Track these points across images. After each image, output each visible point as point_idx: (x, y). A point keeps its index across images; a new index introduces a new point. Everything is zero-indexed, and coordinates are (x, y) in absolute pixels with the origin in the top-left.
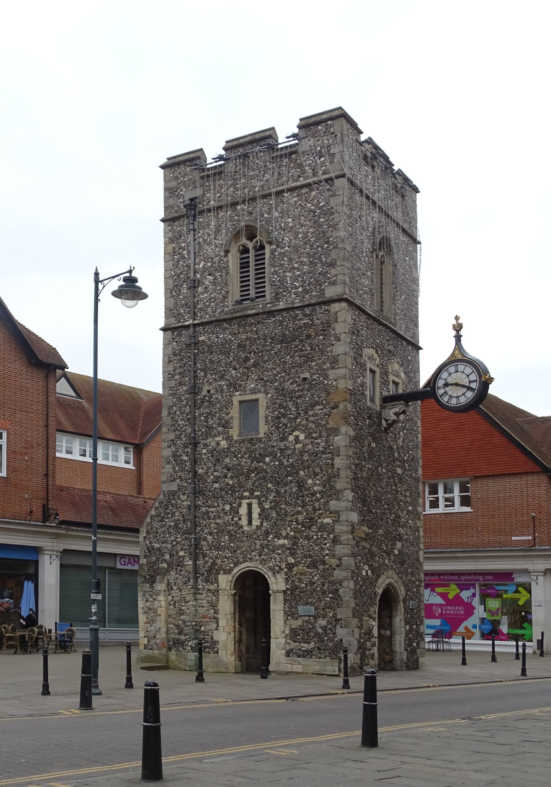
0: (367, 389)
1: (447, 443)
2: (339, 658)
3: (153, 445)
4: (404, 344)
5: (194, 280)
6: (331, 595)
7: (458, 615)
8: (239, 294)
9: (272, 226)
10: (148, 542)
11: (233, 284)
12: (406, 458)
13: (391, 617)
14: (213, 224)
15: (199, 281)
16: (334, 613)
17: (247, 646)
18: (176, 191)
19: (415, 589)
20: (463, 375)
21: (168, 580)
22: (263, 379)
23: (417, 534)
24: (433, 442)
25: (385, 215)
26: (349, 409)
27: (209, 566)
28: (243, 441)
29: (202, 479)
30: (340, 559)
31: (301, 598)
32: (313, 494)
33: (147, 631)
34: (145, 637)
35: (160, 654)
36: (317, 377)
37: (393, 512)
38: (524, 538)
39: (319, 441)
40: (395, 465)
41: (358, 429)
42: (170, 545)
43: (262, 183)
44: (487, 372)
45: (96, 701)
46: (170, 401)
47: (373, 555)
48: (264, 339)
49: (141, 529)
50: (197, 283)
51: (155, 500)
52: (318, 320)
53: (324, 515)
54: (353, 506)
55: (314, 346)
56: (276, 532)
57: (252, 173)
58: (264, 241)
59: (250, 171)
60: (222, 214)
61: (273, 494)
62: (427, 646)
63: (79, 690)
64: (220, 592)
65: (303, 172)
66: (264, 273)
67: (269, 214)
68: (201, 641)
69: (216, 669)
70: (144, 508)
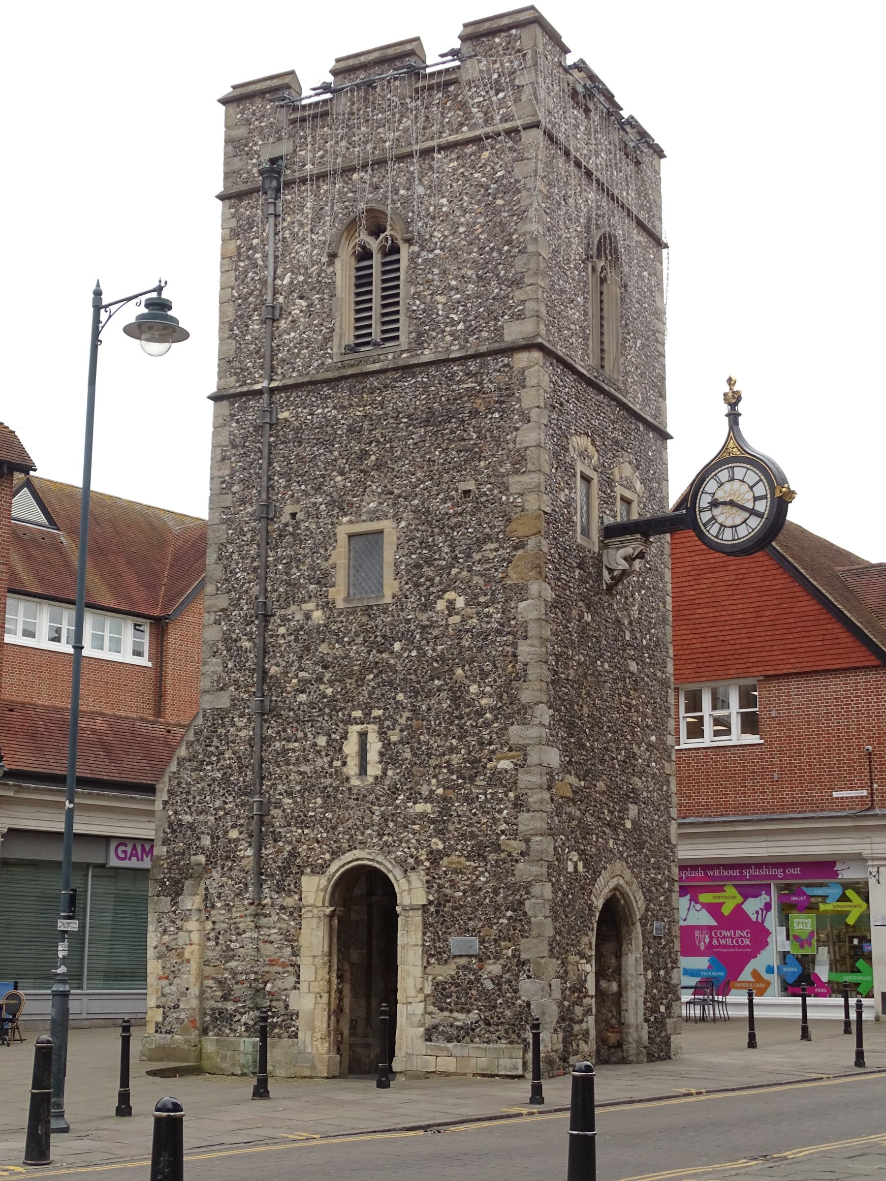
0: (576, 513)
1: (716, 614)
2: (525, 1040)
3: (188, 618)
4: (642, 428)
5: (273, 307)
6: (509, 913)
7: (739, 947)
8: (353, 333)
9: (413, 212)
10: (170, 813)
11: (341, 314)
12: (644, 643)
13: (619, 956)
14: (309, 205)
15: (281, 309)
16: (515, 950)
17: (351, 1021)
18: (246, 145)
19: (662, 898)
20: (743, 487)
21: (206, 889)
22: (392, 493)
23: (665, 788)
24: (692, 612)
25: (608, 194)
26: (545, 550)
27: (285, 859)
28: (353, 611)
29: (277, 684)
30: (527, 841)
31: (455, 920)
32: (480, 713)
33: (163, 995)
34: (158, 1007)
35: (187, 1041)
36: (488, 489)
37: (622, 746)
38: (854, 793)
39: (491, 610)
40: (625, 655)
41: (560, 585)
42: (213, 818)
43: (397, 134)
44: (784, 481)
45: (58, 1145)
46: (223, 533)
47: (587, 832)
48: (396, 418)
49: (159, 786)
50: (277, 312)
51: (187, 727)
52: (491, 382)
53: (498, 755)
54: (552, 735)
55: (483, 431)
56: (411, 788)
57: (380, 116)
58: (399, 238)
59: (376, 112)
60: (325, 187)
61: (407, 714)
62: (684, 1012)
63: (26, 1123)
64: (303, 911)
65: (468, 116)
66: (398, 295)
67: (408, 189)
68: (266, 1012)
69: (292, 1071)
70: (166, 743)
